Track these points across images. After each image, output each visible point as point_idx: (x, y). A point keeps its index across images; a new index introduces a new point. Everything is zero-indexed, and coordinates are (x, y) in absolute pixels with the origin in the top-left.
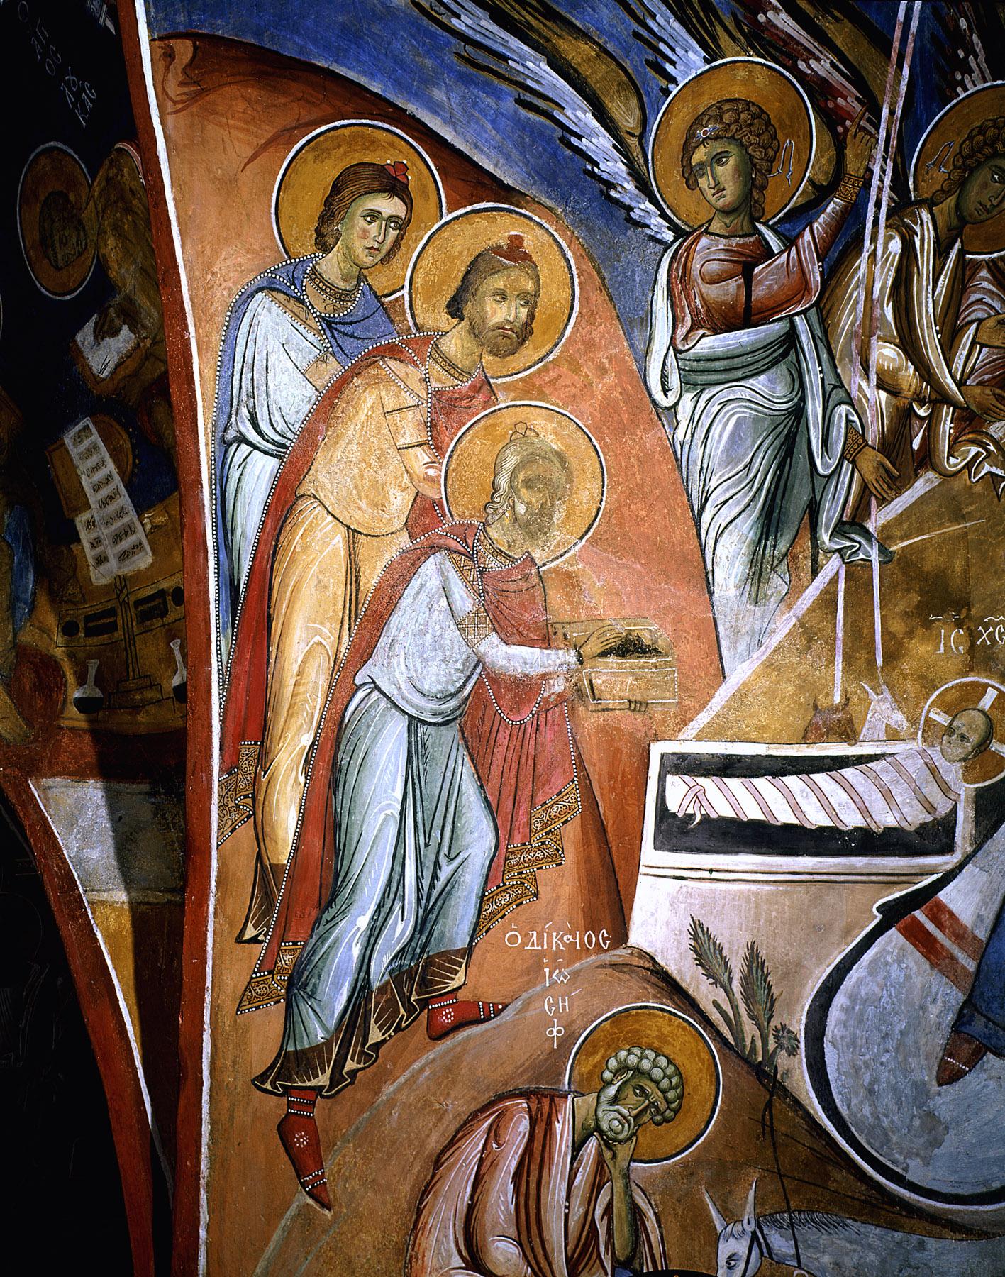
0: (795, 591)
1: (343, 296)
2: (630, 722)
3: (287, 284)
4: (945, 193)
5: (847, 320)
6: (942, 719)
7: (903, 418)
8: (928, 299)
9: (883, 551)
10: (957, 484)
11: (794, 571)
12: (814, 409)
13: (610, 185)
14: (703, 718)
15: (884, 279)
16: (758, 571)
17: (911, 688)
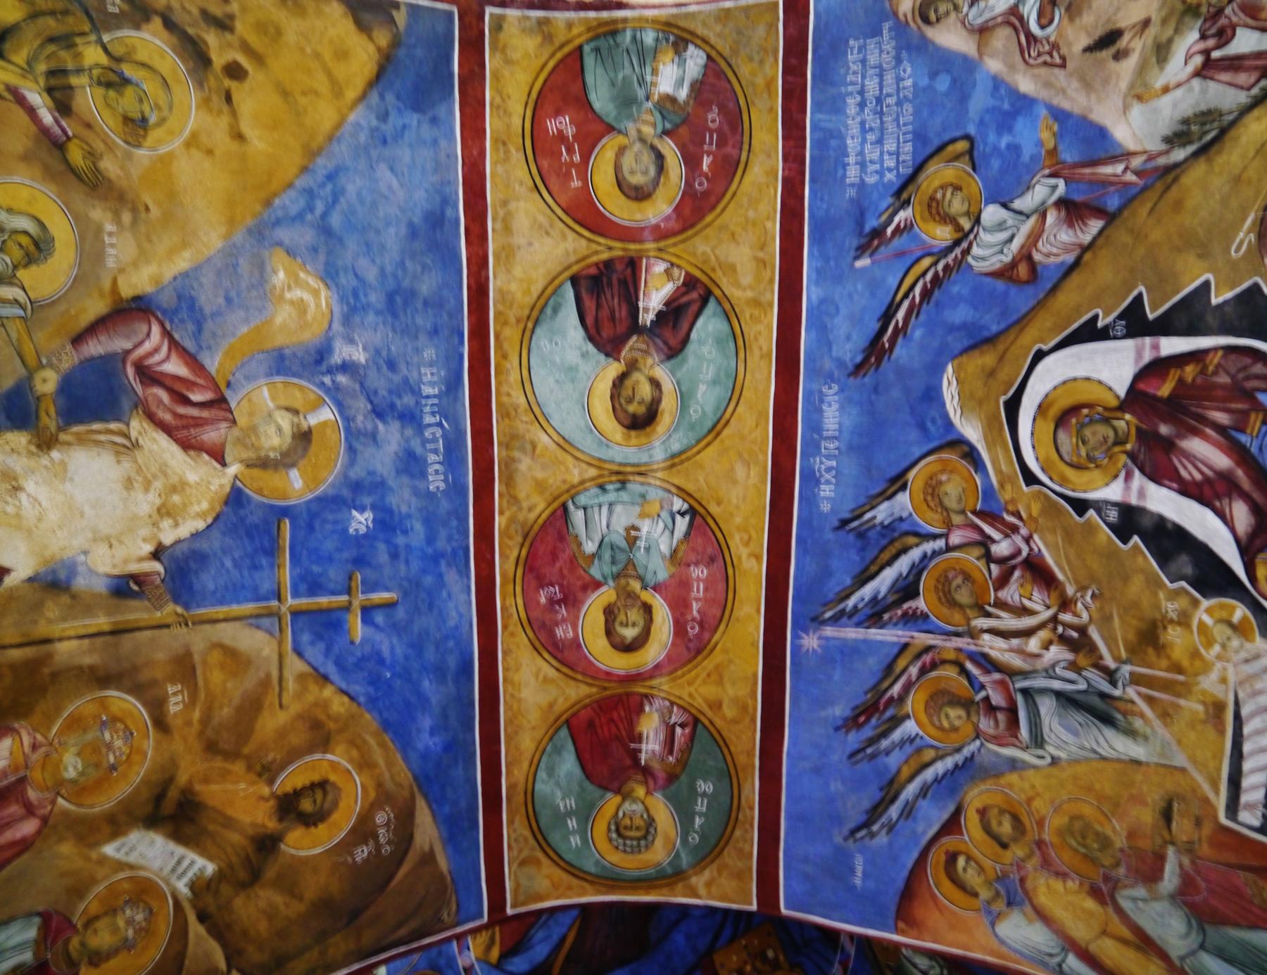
0: (1142, 715)
1: (998, 894)
2: (1207, 830)
3: (995, 919)
4: (965, 614)
5: (1017, 662)
6: (1217, 648)
7: (1063, 640)
8: (1009, 622)
9: (1124, 662)
10: (1095, 616)
11: (1133, 714)
12: (1057, 685)
13: (956, 766)
14: (1206, 788)
15: (1000, 643)
16: (1131, 733)
17: (1198, 663)
